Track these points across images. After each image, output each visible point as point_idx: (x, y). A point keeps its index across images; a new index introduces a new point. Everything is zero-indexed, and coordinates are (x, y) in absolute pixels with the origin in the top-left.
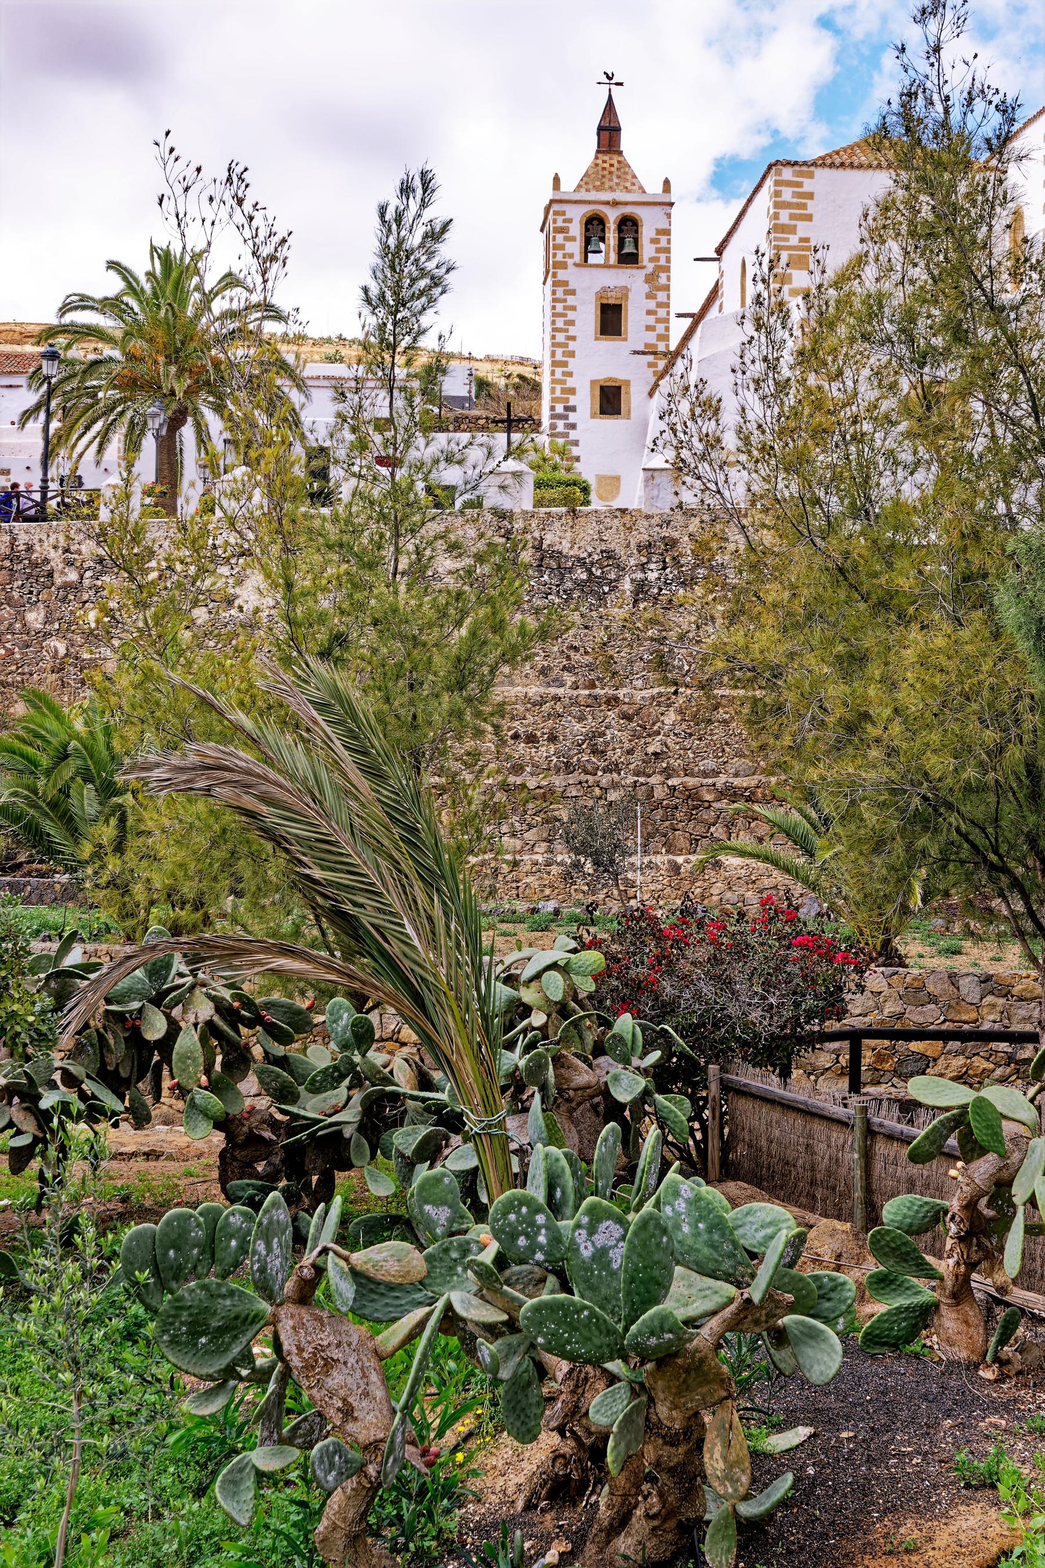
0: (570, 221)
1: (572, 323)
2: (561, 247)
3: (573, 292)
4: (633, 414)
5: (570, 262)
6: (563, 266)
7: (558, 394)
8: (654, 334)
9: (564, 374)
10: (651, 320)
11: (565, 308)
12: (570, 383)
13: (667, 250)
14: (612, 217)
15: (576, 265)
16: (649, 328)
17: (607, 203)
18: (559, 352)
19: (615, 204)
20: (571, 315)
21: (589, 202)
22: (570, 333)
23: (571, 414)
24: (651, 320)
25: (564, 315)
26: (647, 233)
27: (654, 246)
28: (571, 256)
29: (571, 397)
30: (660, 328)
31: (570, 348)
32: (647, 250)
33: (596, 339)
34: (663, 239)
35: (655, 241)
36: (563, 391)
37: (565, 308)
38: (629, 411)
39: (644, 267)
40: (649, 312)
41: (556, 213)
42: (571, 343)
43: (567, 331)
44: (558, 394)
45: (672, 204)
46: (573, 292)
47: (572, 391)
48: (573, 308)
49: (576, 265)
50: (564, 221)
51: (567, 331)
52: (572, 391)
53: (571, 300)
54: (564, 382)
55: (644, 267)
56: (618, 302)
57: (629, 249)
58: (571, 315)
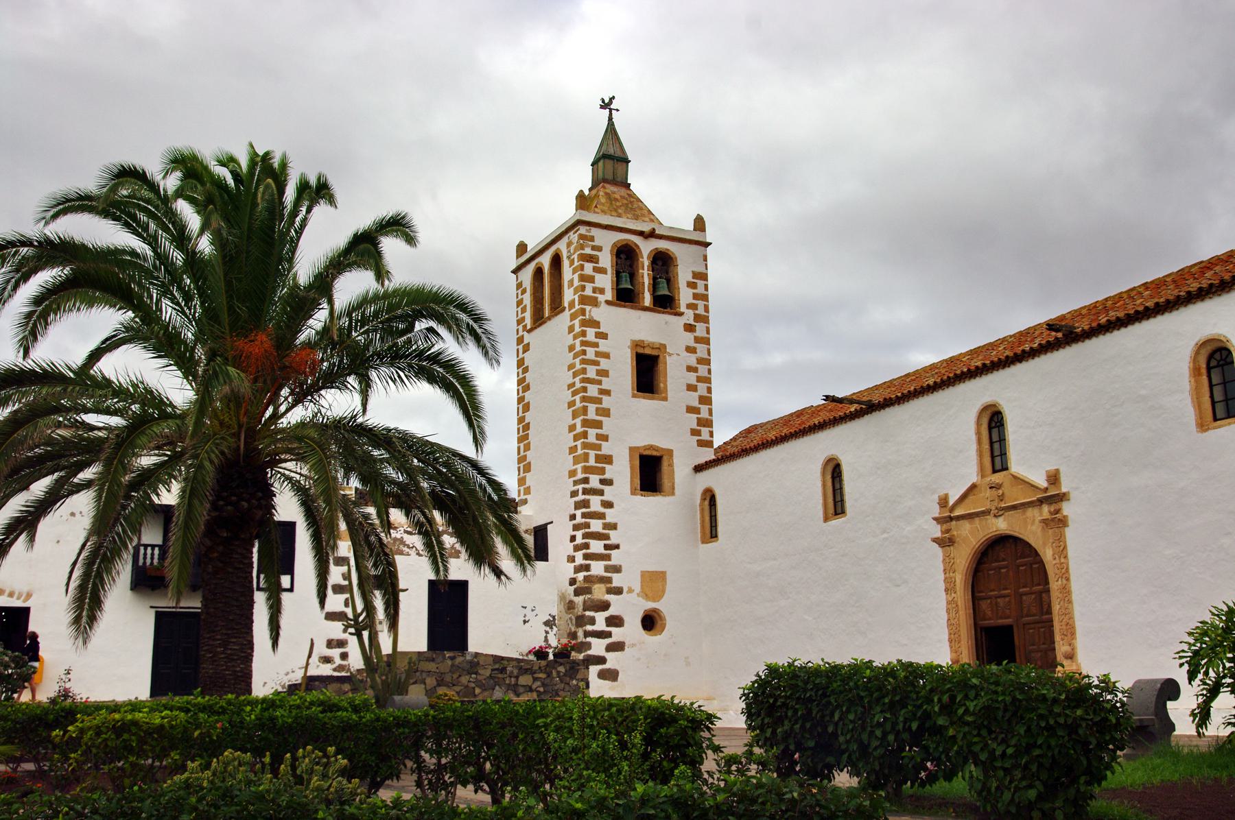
0: (599, 249)
1: (604, 373)
2: (591, 279)
3: (604, 336)
4: (676, 491)
5: (601, 298)
6: (594, 302)
7: (592, 462)
8: (696, 395)
9: (599, 437)
10: (692, 378)
11: (597, 354)
12: (606, 449)
13: (705, 298)
14: (646, 248)
15: (608, 302)
16: (692, 388)
17: (641, 234)
18: (592, 408)
19: (652, 235)
20: (604, 364)
21: (621, 230)
22: (603, 387)
23: (607, 489)
24: (692, 378)
25: (596, 363)
26: (683, 275)
27: (691, 291)
28: (602, 291)
29: (607, 467)
30: (702, 388)
31: (605, 405)
32: (685, 296)
33: (634, 396)
34: (700, 283)
35: (692, 285)
36: (599, 459)
37: (597, 354)
38: (674, 489)
39: (681, 314)
40: (690, 369)
41: (582, 237)
42: (605, 398)
43: (600, 383)
44: (592, 462)
45: (707, 245)
46: (604, 336)
47: (608, 459)
48: (606, 356)
49: (608, 302)
50: (594, 248)
51: (600, 383)
52: (608, 459)
53: (604, 346)
54: (598, 447)
55: (681, 314)
56: (655, 353)
57: (664, 291)
58: (604, 364)
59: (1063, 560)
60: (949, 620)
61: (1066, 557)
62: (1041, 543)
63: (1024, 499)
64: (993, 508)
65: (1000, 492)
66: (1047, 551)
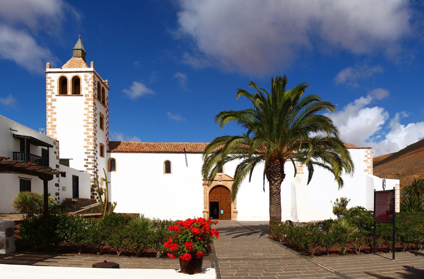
35: (107, 100)
60: (204, 200)
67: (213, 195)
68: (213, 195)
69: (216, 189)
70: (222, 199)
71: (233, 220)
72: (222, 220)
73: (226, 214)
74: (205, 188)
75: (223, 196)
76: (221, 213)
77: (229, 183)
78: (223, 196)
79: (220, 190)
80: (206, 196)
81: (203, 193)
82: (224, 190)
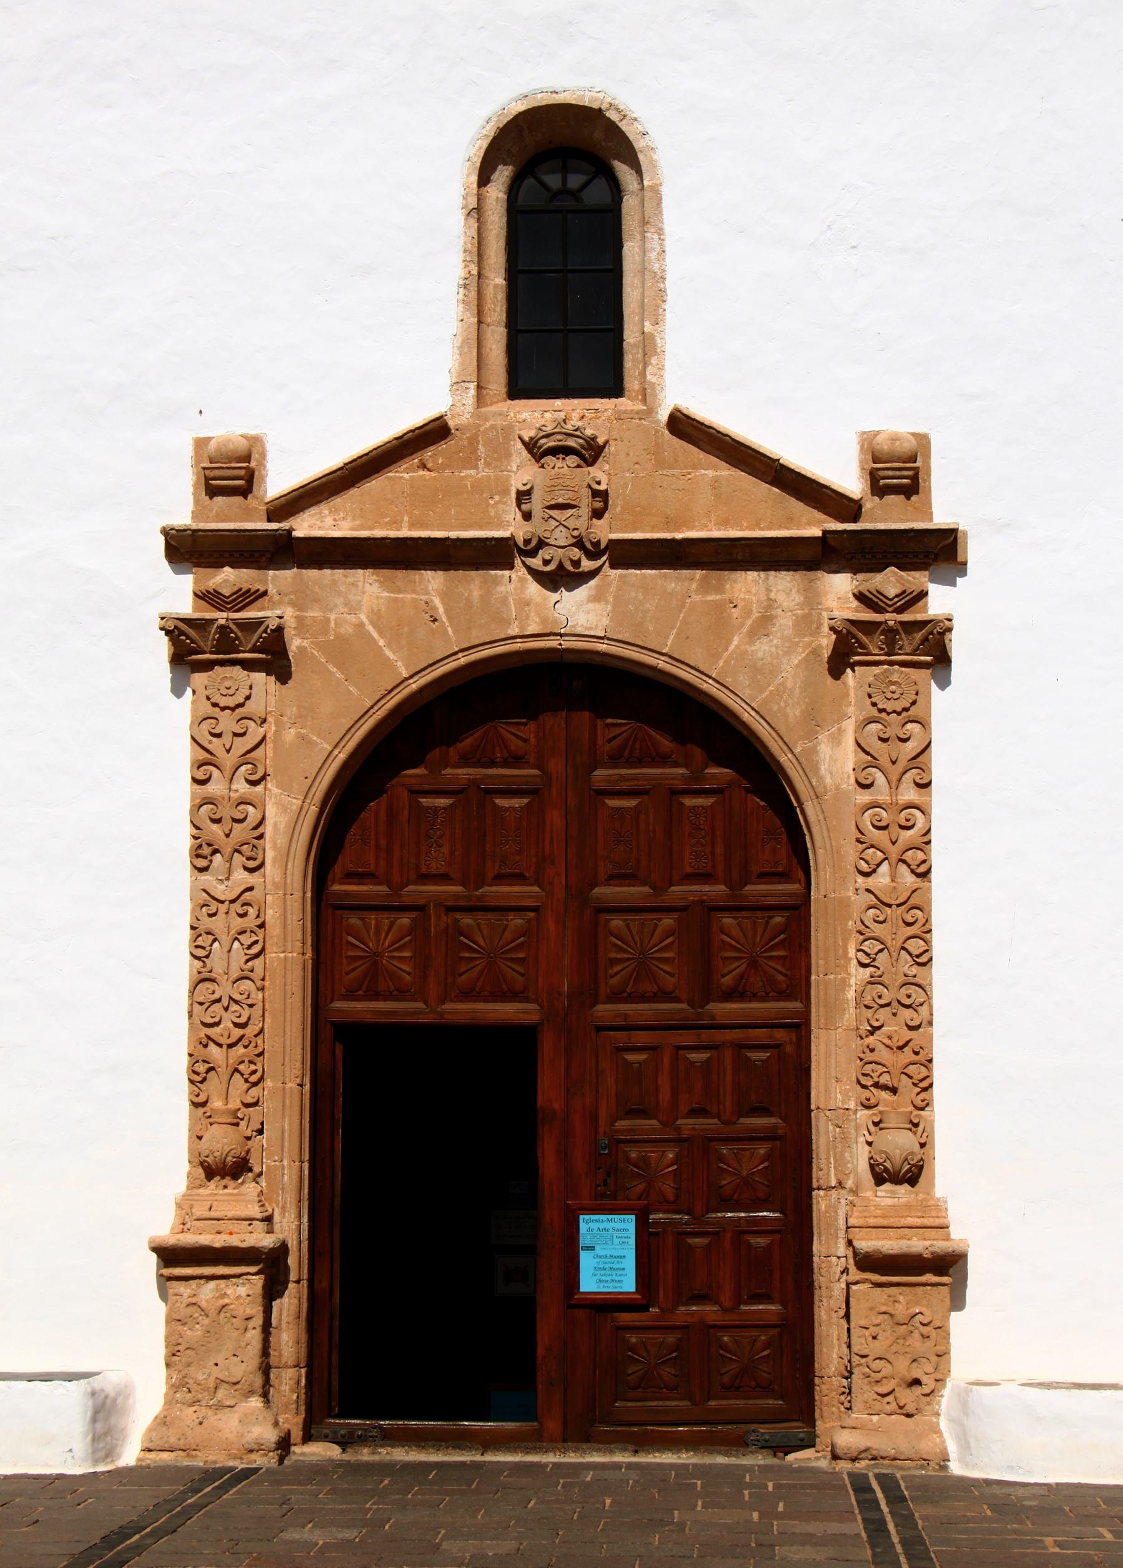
59: (909, 794)
60: (202, 979)
61: (924, 786)
62: (795, 713)
63: (725, 523)
64: (561, 537)
65: (599, 473)
66: (825, 750)
67: (416, 892)
68: (416, 892)
69: (466, 760)
70: (617, 975)
71: (846, 1440)
72: (607, 1442)
73: (709, 1311)
74: (227, 722)
75: (638, 892)
76: (589, 1282)
77: (766, 620)
78: (638, 892)
79: (556, 766)
80: (242, 900)
81: (185, 843)
82: (664, 760)
